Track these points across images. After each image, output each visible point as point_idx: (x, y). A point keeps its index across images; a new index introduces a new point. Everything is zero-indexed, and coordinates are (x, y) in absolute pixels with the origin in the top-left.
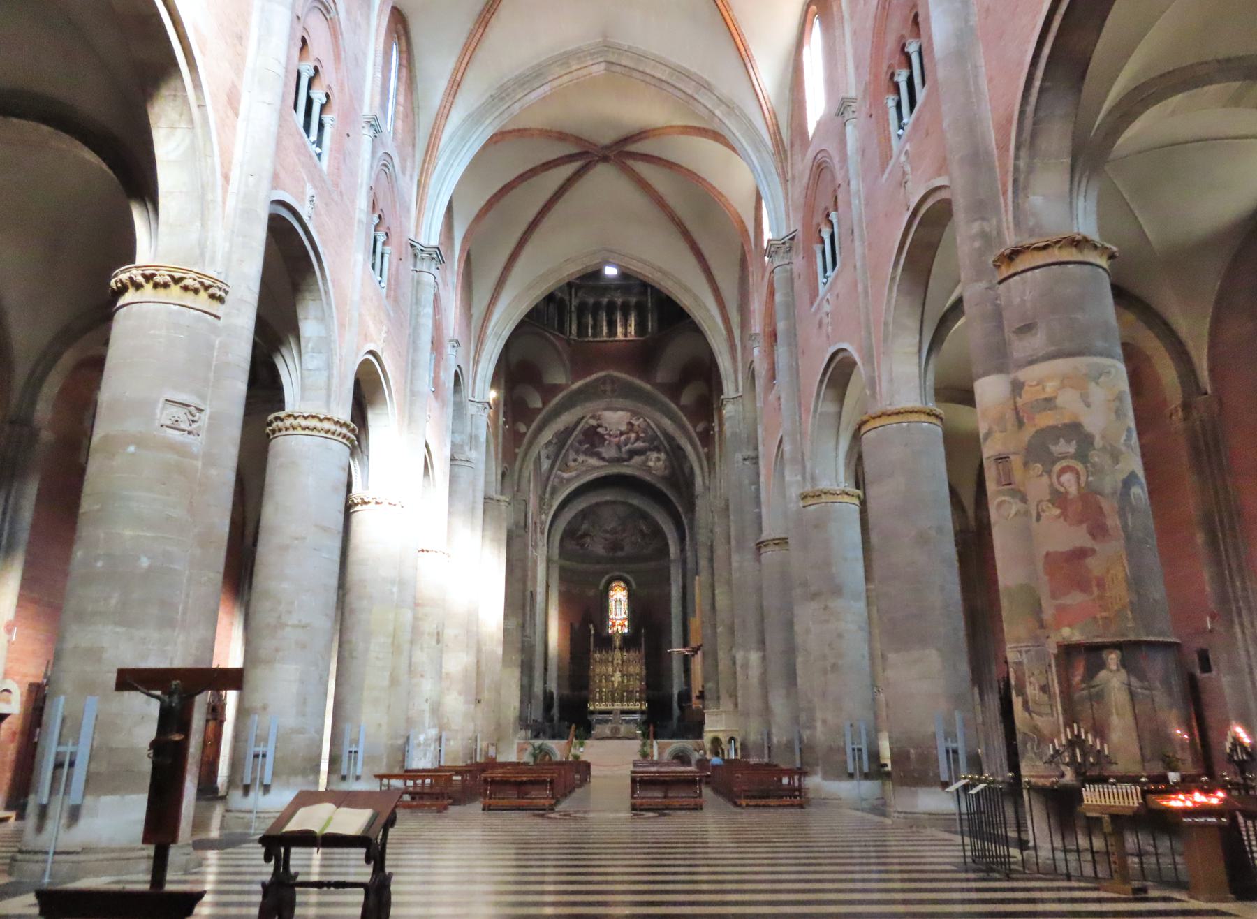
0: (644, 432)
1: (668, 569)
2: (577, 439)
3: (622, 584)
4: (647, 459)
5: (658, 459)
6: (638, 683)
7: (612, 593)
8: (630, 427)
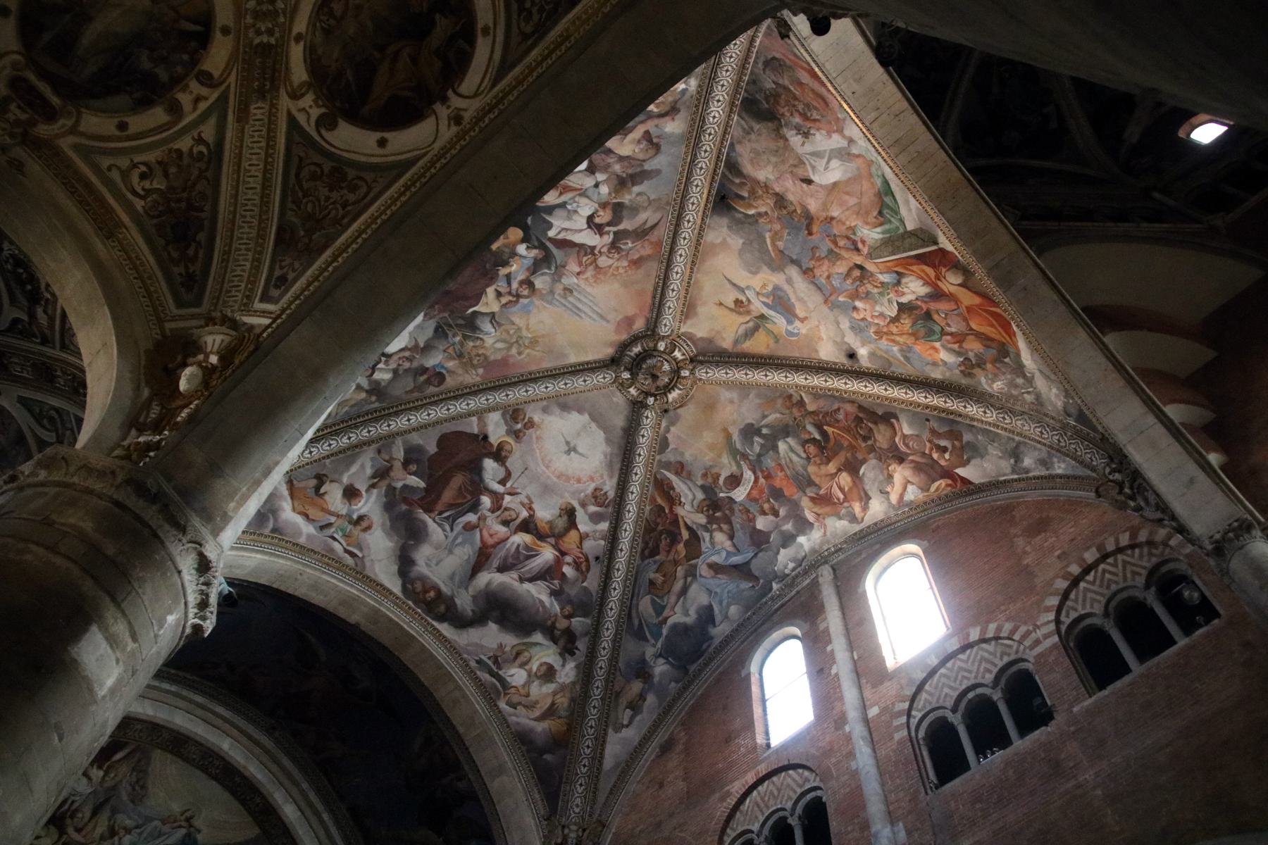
0: (577, 565)
2: (416, 439)
4: (517, 656)
5: (549, 673)
8: (561, 523)
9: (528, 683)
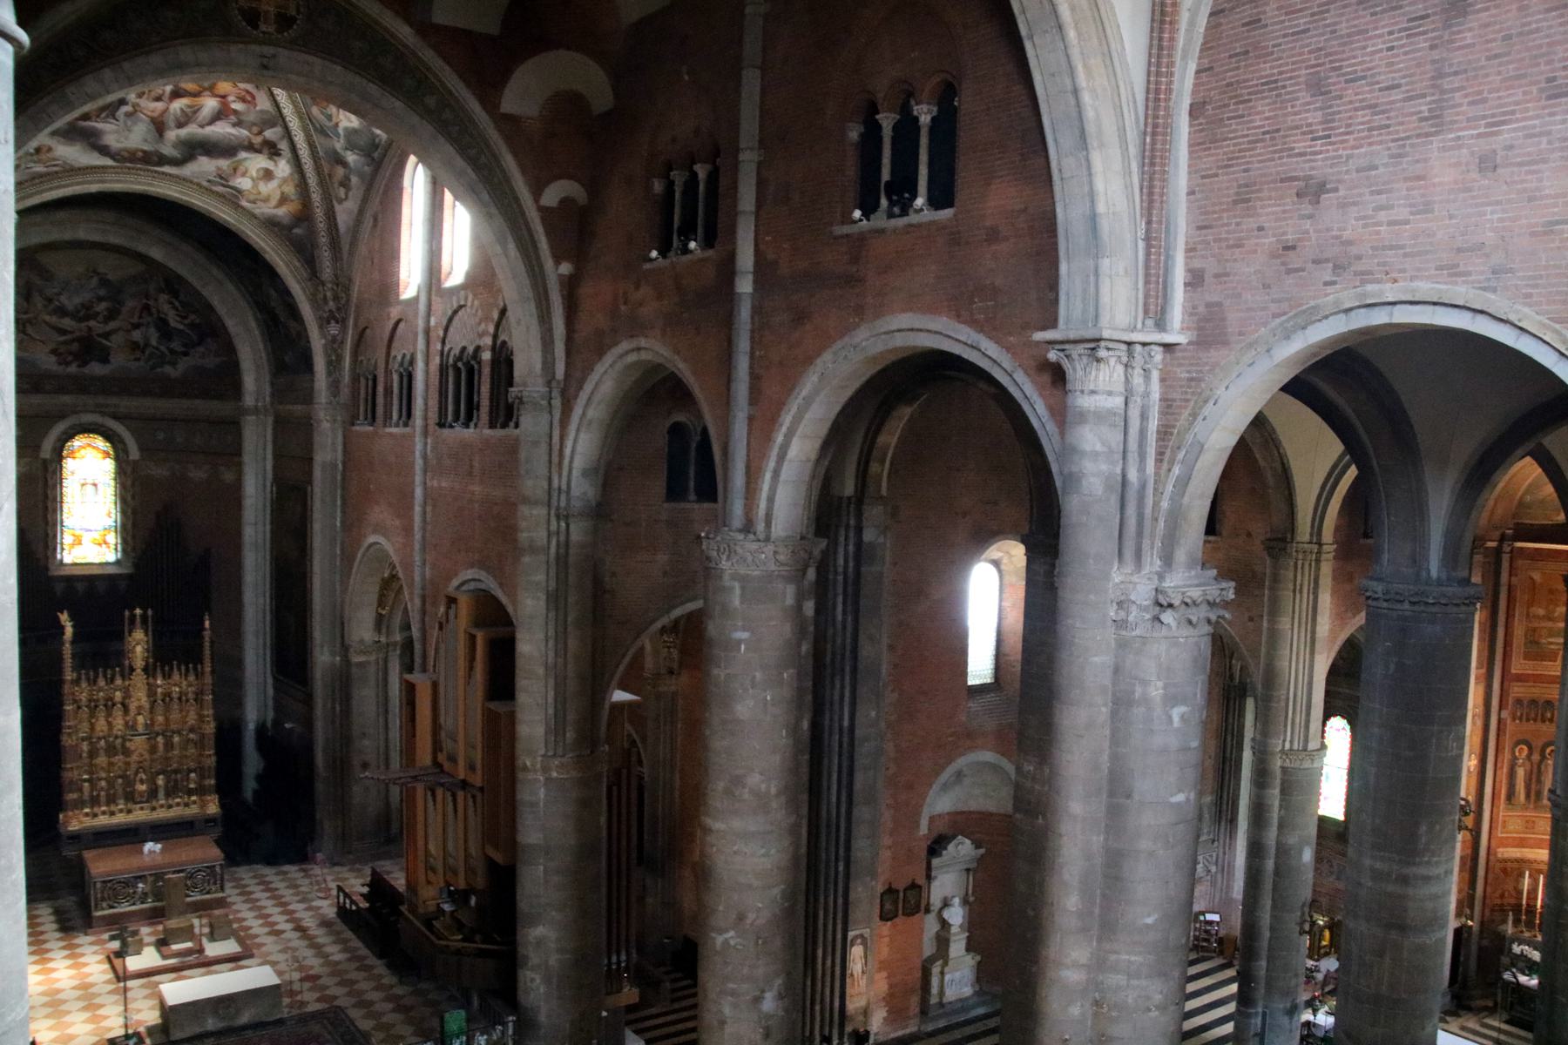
1: (233, 426)
3: (100, 443)
5: (268, 175)
6: (192, 751)
7: (69, 465)
9: (255, 185)
